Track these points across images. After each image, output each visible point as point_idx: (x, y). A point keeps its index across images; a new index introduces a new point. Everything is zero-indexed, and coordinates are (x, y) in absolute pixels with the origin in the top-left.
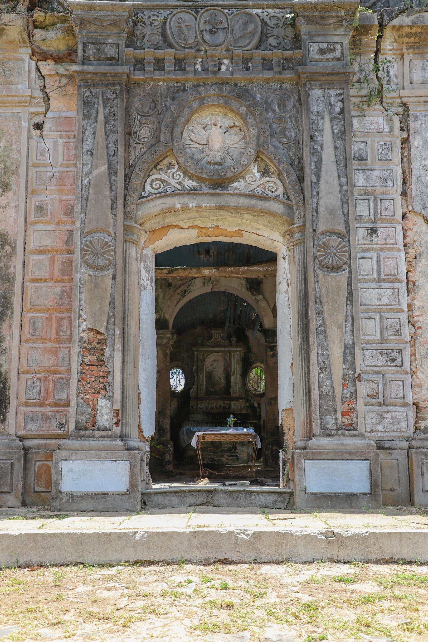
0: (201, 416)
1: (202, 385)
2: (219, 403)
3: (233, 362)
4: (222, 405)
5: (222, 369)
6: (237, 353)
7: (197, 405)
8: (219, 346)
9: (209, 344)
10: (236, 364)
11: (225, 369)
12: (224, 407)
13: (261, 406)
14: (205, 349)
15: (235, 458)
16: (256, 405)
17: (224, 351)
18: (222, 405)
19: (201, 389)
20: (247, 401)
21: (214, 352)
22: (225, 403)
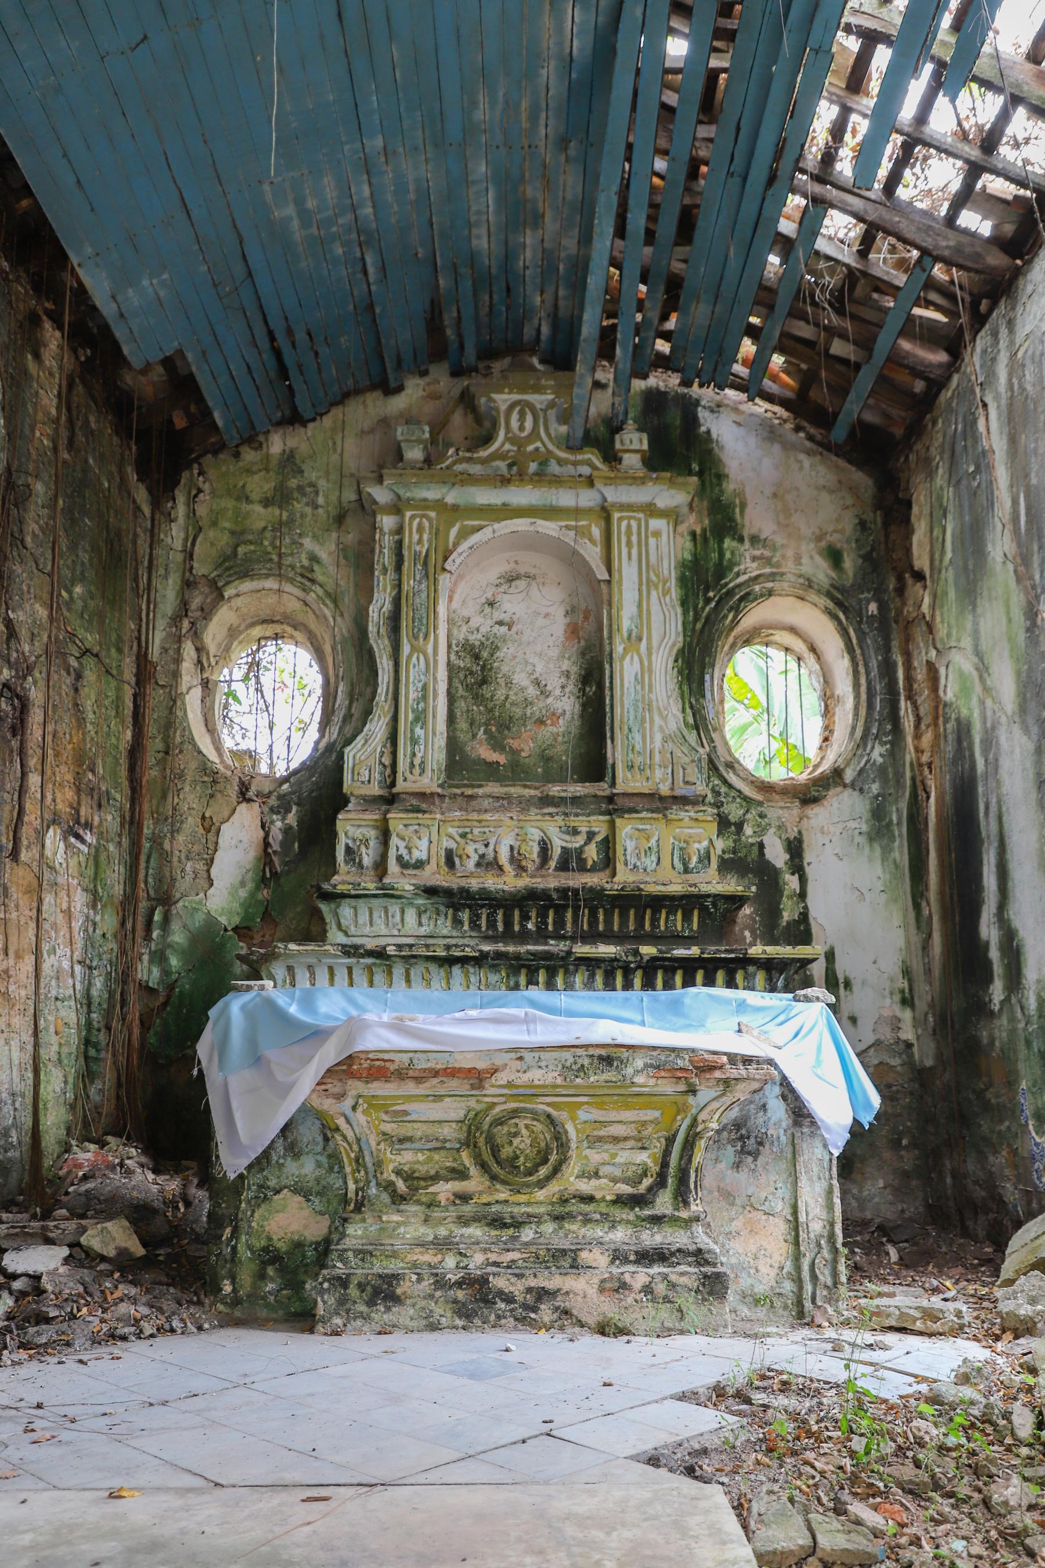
0: (411, 915)
1: (420, 718)
2: (535, 834)
3: (628, 574)
4: (558, 843)
5: (559, 625)
6: (656, 524)
7: (385, 835)
8: (541, 478)
9: (476, 469)
10: (645, 586)
11: (573, 631)
12: (571, 860)
13: (808, 856)
14: (452, 497)
15: (685, 1274)
16: (777, 855)
17: (576, 512)
18: (558, 843)
19: (414, 741)
20: (724, 823)
21: (507, 512)
22: (575, 832)
